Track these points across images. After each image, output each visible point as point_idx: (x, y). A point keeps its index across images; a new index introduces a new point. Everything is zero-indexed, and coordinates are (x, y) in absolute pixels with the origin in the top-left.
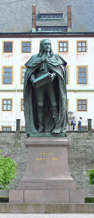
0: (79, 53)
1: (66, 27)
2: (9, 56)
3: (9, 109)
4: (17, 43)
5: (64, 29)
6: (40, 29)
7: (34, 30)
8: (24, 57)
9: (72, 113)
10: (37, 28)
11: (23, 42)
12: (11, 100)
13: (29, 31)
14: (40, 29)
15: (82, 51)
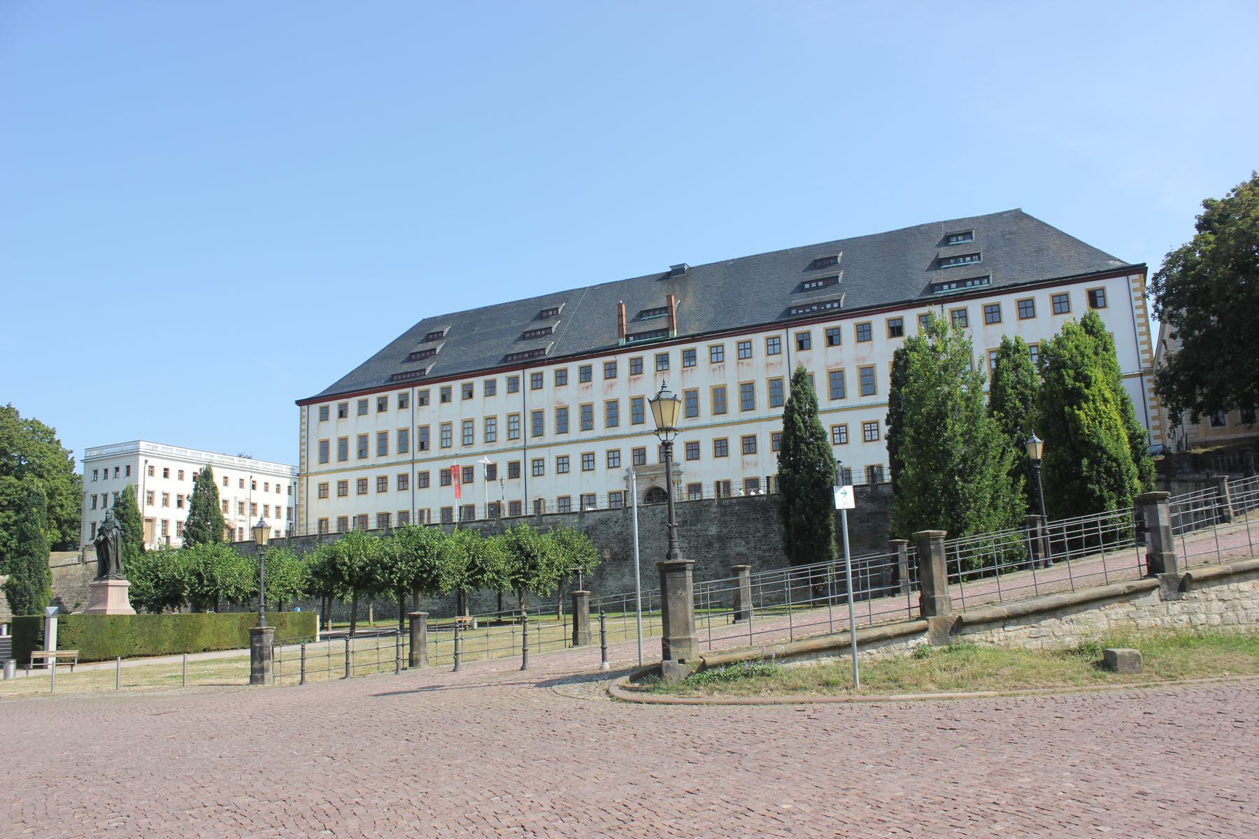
0: (685, 369)
1: (667, 330)
2: (587, 387)
3: (591, 467)
4: (598, 365)
5: (666, 333)
6: (631, 338)
7: (623, 342)
8: (608, 386)
9: (678, 465)
10: (627, 337)
11: (631, 360)
12: (593, 454)
13: (613, 343)
14: (631, 338)
15: (690, 366)
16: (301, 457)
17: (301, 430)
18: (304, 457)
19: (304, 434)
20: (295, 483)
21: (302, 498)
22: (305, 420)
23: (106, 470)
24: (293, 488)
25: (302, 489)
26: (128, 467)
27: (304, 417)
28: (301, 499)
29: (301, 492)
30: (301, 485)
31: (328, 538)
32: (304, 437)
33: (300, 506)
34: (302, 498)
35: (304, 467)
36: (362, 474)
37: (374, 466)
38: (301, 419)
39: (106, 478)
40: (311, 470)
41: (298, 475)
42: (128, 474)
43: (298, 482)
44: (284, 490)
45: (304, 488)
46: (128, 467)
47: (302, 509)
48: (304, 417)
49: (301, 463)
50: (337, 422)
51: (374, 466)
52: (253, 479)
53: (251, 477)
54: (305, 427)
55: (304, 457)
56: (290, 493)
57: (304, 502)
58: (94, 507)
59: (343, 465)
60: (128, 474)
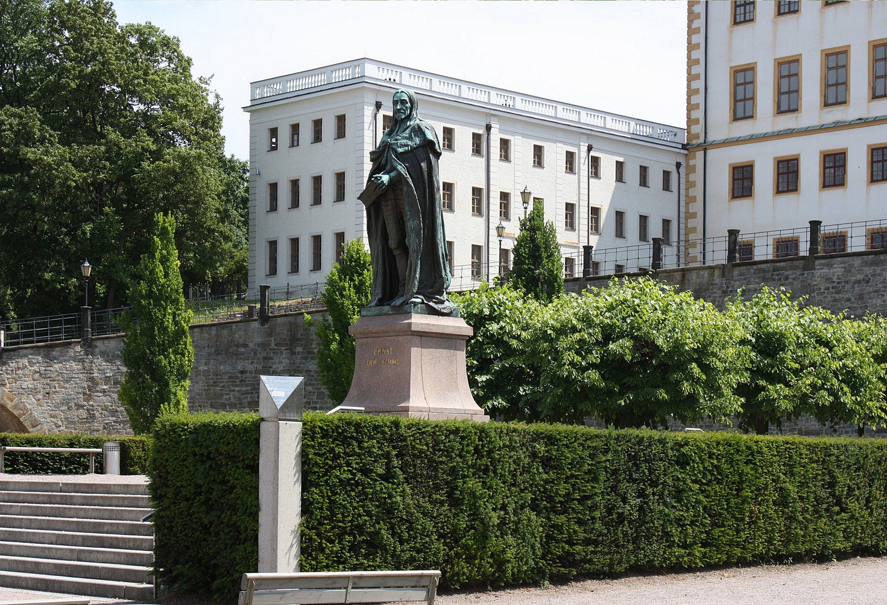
16: (690, 107)
17: (691, 47)
18: (697, 106)
19: (699, 54)
20: (678, 165)
21: (694, 199)
22: (700, 23)
23: (295, 128)
24: (674, 177)
25: (692, 177)
26: (341, 120)
27: (698, 16)
28: (691, 200)
29: (691, 185)
30: (691, 169)
31: (830, 266)
32: (697, 62)
33: (690, 216)
34: (694, 199)
35: (698, 129)
36: (833, 142)
37: (862, 122)
38: (690, 21)
39: (294, 142)
40: (711, 138)
41: (684, 147)
42: (341, 133)
43: (684, 164)
44: (655, 178)
45: (697, 177)
46: (341, 120)
47: (691, 223)
48: (698, 16)
49: (690, 121)
50: (775, 24)
51: (862, 122)
52: (592, 153)
53: (590, 148)
54: (699, 39)
55: (697, 106)
56: (666, 187)
57: (697, 207)
58: (274, 207)
59: (787, 122)
60: (341, 133)
